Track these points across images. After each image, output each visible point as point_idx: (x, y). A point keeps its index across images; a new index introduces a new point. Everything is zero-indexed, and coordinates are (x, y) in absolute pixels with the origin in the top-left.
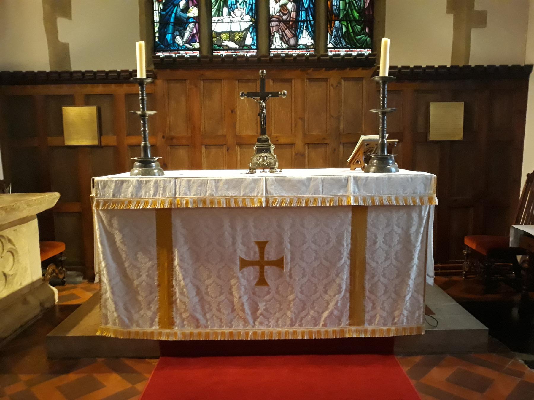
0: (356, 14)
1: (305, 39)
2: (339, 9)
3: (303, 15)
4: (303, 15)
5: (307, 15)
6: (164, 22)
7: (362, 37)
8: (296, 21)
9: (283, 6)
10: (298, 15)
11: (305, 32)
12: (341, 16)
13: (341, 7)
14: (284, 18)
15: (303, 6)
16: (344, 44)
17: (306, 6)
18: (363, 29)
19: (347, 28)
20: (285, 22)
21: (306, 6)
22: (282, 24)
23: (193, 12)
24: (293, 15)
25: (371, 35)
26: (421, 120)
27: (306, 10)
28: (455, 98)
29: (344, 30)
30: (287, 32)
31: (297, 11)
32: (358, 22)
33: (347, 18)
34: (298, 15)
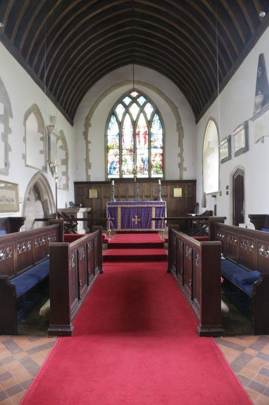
1: (146, 172)
6: (111, 168)
26: (172, 192)
28: (180, 187)
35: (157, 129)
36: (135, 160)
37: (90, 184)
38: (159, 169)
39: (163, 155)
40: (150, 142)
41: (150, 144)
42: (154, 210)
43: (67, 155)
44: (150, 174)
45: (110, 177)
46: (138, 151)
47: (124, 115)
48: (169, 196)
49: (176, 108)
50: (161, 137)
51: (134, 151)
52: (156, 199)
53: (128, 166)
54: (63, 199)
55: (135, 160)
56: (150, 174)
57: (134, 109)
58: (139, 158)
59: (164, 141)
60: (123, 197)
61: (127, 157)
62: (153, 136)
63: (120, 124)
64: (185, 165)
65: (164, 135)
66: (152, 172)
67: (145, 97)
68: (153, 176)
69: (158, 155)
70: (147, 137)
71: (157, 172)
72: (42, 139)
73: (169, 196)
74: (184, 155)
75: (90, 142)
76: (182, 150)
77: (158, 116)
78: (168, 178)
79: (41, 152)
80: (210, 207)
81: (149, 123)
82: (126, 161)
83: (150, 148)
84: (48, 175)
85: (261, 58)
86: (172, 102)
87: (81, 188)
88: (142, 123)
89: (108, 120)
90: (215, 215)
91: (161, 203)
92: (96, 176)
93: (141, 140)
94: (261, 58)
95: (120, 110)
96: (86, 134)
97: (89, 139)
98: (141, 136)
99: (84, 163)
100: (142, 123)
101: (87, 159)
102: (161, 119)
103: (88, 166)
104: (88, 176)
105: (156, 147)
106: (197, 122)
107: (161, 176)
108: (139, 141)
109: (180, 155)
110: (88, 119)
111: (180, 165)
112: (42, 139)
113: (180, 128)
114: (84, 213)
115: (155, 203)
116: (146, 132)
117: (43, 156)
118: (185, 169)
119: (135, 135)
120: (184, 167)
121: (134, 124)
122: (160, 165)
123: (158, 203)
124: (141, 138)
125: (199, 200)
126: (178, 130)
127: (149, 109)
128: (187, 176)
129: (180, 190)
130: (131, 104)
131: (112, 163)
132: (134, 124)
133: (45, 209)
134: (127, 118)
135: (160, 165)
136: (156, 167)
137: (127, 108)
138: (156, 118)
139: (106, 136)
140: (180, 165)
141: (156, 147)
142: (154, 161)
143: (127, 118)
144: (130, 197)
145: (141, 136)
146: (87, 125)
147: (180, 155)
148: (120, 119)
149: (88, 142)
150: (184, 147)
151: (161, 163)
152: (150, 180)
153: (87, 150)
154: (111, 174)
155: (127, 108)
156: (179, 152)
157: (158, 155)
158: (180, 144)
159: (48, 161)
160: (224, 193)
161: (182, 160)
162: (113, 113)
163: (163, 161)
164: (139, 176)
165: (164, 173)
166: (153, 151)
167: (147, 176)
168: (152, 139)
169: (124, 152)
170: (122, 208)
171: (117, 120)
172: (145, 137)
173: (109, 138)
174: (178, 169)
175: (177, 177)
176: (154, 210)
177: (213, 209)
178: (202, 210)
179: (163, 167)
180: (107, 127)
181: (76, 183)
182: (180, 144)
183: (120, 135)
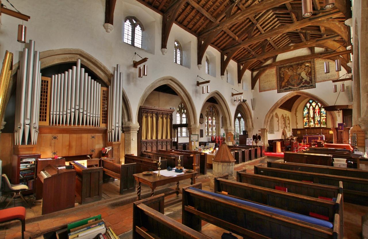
1: (319, 125)
6: (305, 124)
23: (308, 123)
36: (314, 121)
37: (298, 130)
39: (326, 119)
40: (321, 115)
43: (290, 121)
44: (321, 126)
45: (305, 127)
46: (316, 118)
47: (310, 106)
48: (328, 133)
51: (314, 118)
53: (312, 124)
54: (289, 134)
55: (314, 121)
56: (321, 126)
57: (314, 104)
58: (316, 120)
59: (326, 114)
60: (309, 133)
61: (312, 120)
63: (309, 109)
66: (322, 125)
71: (324, 125)
72: (284, 121)
73: (328, 133)
75: (297, 116)
79: (284, 124)
81: (320, 109)
82: (311, 121)
83: (320, 117)
84: (285, 129)
87: (295, 131)
88: (317, 108)
89: (304, 108)
92: (300, 126)
95: (308, 105)
96: (296, 114)
97: (297, 116)
98: (317, 113)
99: (295, 123)
100: (317, 108)
101: (296, 122)
103: (297, 124)
104: (297, 127)
105: (323, 116)
107: (325, 126)
108: (316, 115)
110: (296, 109)
112: (284, 121)
114: (296, 138)
117: (284, 125)
119: (314, 113)
121: (314, 109)
124: (317, 115)
130: (312, 102)
131: (306, 122)
132: (314, 109)
133: (285, 137)
134: (311, 107)
137: (311, 104)
139: (303, 113)
141: (323, 116)
143: (311, 107)
144: (312, 133)
145: (317, 113)
146: (296, 111)
148: (308, 107)
149: (296, 117)
153: (296, 119)
154: (305, 126)
155: (311, 104)
159: (285, 126)
162: (306, 106)
164: (316, 126)
166: (322, 118)
167: (319, 126)
169: (311, 118)
170: (308, 137)
171: (307, 108)
172: (318, 113)
173: (304, 114)
179: (326, 123)
180: (304, 111)
181: (293, 129)
183: (309, 113)
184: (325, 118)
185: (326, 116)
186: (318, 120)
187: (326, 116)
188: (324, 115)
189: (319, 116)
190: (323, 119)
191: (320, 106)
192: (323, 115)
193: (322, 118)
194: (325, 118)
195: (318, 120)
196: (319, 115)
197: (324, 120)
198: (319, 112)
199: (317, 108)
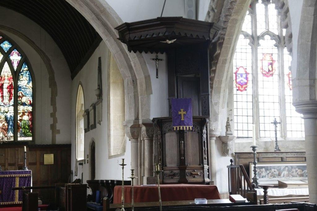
0: (27, 127)
1: (11, 134)
2: (21, 125)
3: (10, 127)
4: (10, 127)
5: (11, 127)
7: (29, 133)
8: (8, 129)
9: (4, 124)
10: (8, 127)
11: (10, 132)
12: (22, 127)
13: (22, 125)
14: (4, 128)
15: (10, 124)
16: (23, 135)
17: (11, 124)
18: (29, 131)
19: (24, 131)
20: (4, 129)
21: (11, 124)
22: (3, 130)
24: (7, 127)
25: (32, 133)
27: (11, 126)
29: (23, 131)
30: (5, 132)
31: (8, 126)
32: (28, 129)
33: (24, 128)
34: (8, 127)
35: (24, 82)
38: (28, 131)
39: (32, 113)
40: (16, 97)
41: (17, 100)
42: (17, 180)
44: (15, 136)
48: (38, 163)
49: (49, 60)
50: (29, 91)
52: (21, 167)
56: (15, 136)
59: (34, 96)
62: (20, 90)
64: (58, 126)
65: (34, 89)
66: (19, 135)
67: (11, 42)
68: (20, 139)
69: (26, 114)
70: (13, 91)
71: (25, 135)
73: (38, 163)
74: (58, 115)
76: (55, 109)
77: (26, 66)
78: (38, 142)
80: (79, 177)
81: (16, 75)
83: (16, 105)
85: (100, 58)
86: (44, 53)
90: (82, 183)
91: (26, 172)
93: (4, 95)
94: (100, 58)
98: (5, 91)
102: (30, 69)
105: (24, 104)
106: (73, 77)
107: (30, 139)
109: (53, 115)
111: (53, 127)
113: (53, 84)
115: (19, 173)
116: (11, 85)
118: (58, 132)
120: (57, 129)
122: (29, 126)
123: (22, 173)
125: (73, 168)
126: (50, 86)
127: (15, 58)
128: (60, 139)
129: (52, 155)
135: (29, 126)
136: (24, 128)
138: (25, 68)
140: (53, 127)
141: (24, 104)
142: (21, 120)
147: (53, 115)
150: (58, 106)
151: (30, 123)
152: (16, 145)
156: (52, 111)
157: (26, 114)
158: (53, 103)
160: (86, 162)
161: (55, 121)
163: (32, 120)
165: (33, 136)
166: (21, 108)
168: (20, 94)
172: (10, 92)
174: (50, 132)
175: (48, 141)
176: (17, 180)
177: (81, 178)
178: (75, 178)
179: (32, 128)
182: (53, 103)
184: (30, 109)
185: (31, 105)
186: (6, 117)
187: (31, 105)
188: (27, 99)
189: (12, 102)
190: (24, 114)
191: (15, 66)
192: (24, 100)
193: (21, 108)
194: (30, 109)
195: (6, 117)
196: (10, 99)
197: (26, 118)
198: (10, 87)
199: (6, 75)
